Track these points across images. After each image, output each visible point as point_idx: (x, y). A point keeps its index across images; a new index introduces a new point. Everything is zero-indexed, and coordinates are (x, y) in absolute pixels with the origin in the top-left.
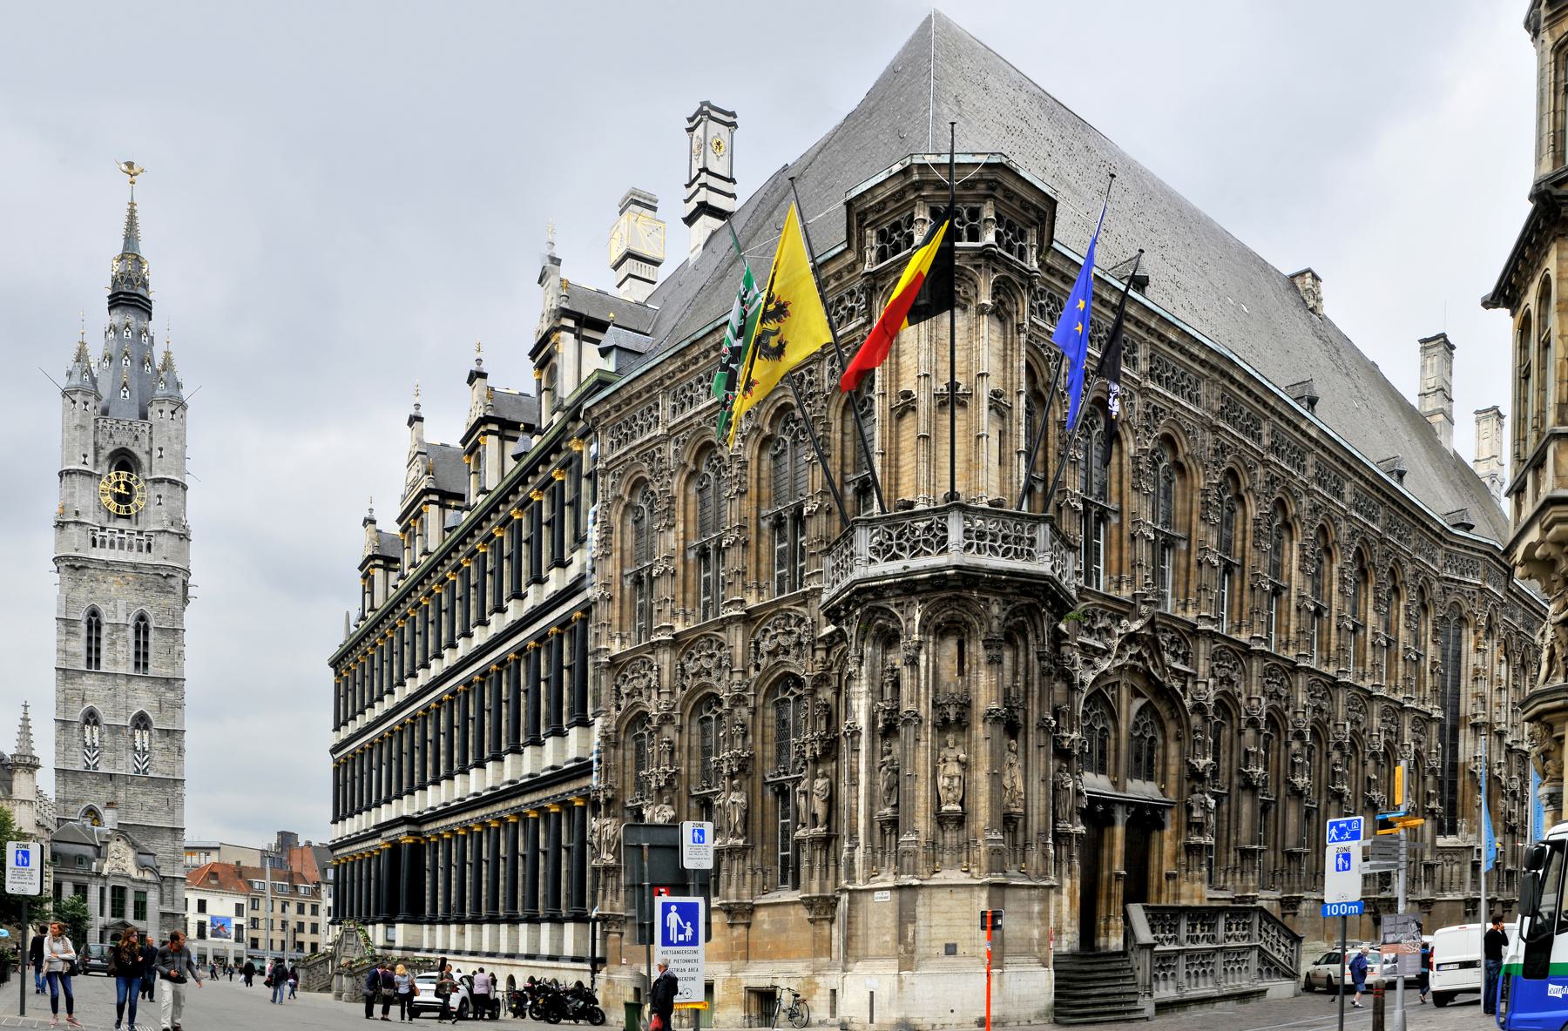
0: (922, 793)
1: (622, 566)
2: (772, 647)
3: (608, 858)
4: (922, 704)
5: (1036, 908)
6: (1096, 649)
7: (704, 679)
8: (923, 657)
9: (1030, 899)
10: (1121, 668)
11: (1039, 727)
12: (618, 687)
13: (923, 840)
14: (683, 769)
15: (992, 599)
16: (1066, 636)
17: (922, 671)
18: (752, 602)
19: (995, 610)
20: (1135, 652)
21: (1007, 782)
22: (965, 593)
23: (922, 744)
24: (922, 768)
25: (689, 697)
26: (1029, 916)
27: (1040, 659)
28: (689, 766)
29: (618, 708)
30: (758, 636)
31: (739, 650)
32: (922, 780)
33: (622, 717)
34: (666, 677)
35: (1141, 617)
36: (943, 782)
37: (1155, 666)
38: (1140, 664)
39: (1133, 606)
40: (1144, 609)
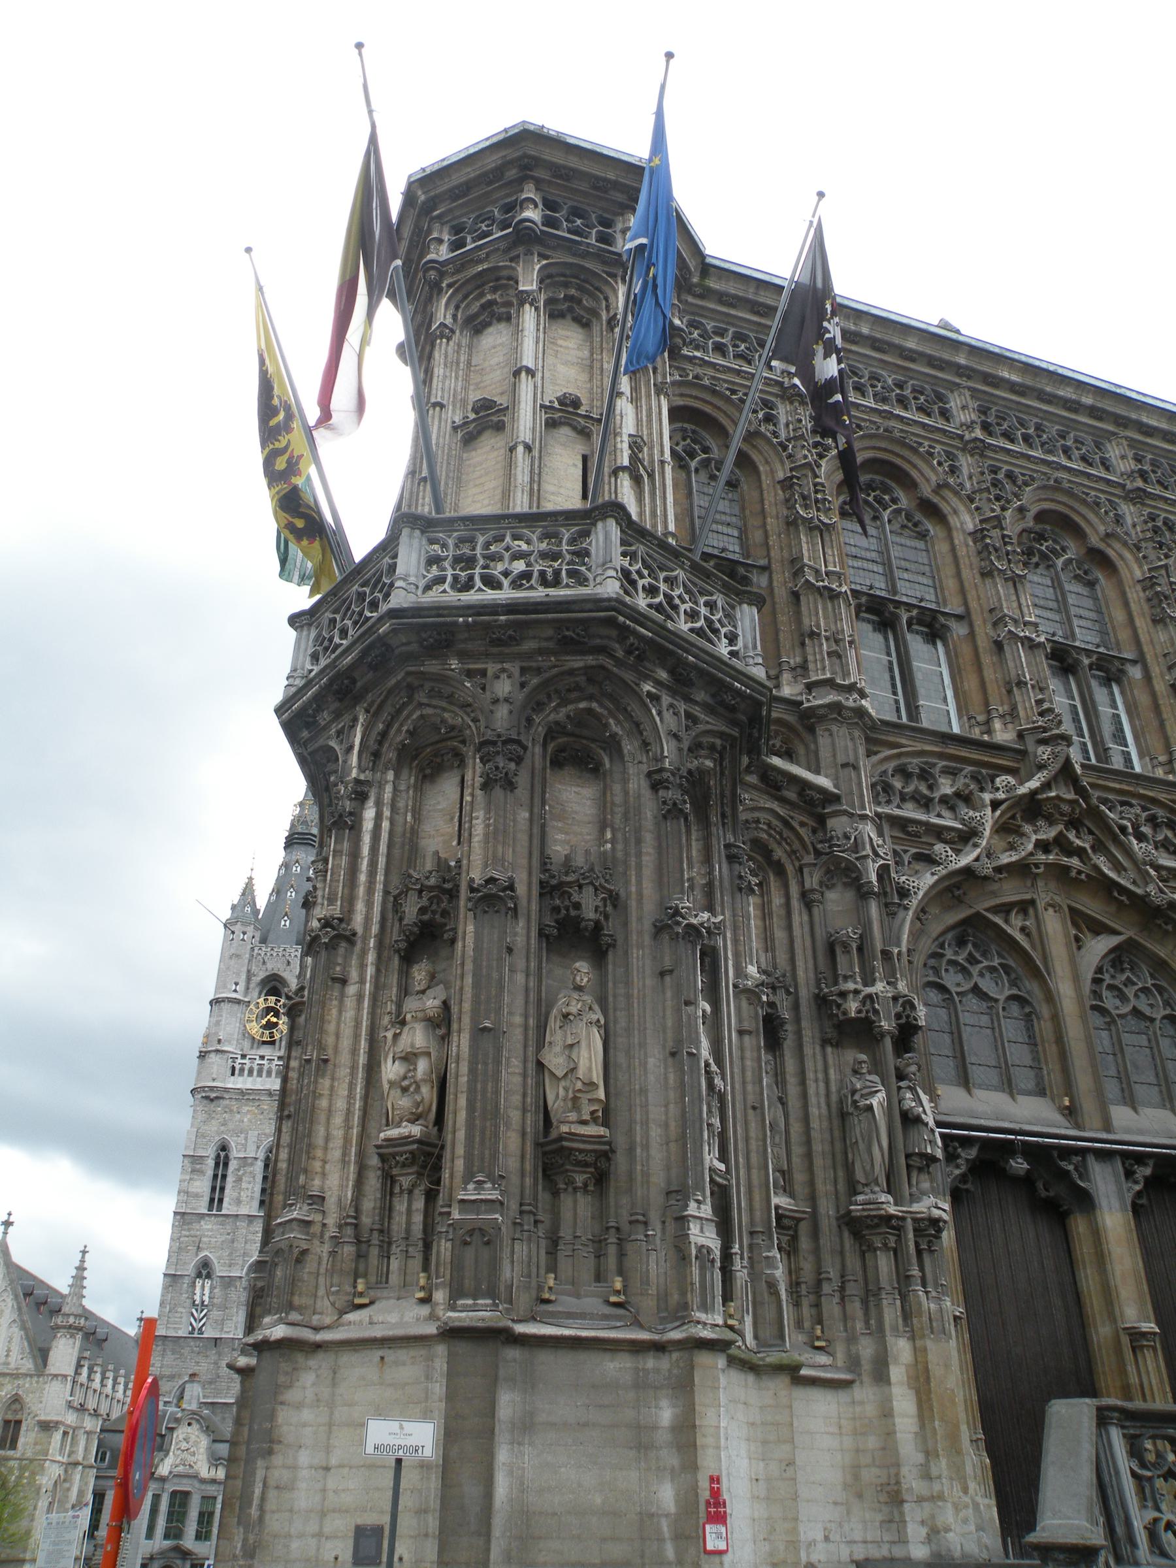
0: (341, 1104)
4: (360, 906)
5: (666, 1414)
6: (939, 833)
8: (369, 814)
9: (641, 1384)
10: (1022, 869)
11: (659, 929)
13: (331, 1220)
15: (492, 668)
16: (836, 799)
17: (366, 839)
19: (504, 687)
20: (1049, 833)
21: (555, 1061)
22: (432, 666)
23: (352, 990)
24: (346, 1043)
26: (641, 1441)
27: (655, 786)
32: (343, 1072)
35: (1041, 767)
36: (391, 1070)
37: (1118, 867)
38: (1075, 862)
39: (1023, 753)
40: (1044, 753)
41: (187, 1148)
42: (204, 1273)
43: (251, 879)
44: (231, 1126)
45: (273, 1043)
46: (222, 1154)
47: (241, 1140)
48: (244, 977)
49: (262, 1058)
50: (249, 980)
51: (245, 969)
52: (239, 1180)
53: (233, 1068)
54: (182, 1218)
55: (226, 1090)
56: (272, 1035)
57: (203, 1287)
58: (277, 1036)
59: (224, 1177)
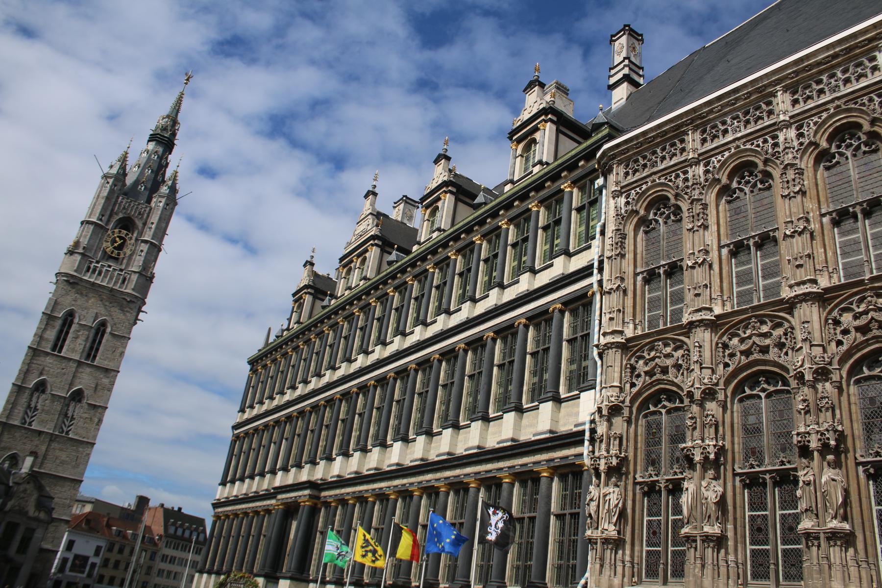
1: (635, 266)
3: (611, 531)
7: (756, 356)
12: (633, 368)
14: (728, 446)
18: (824, 282)
25: (734, 375)
28: (733, 443)
29: (633, 385)
30: (835, 313)
31: (816, 325)
34: (707, 354)
41: (47, 308)
42: (41, 389)
43: (127, 153)
44: (79, 302)
45: (116, 259)
46: (70, 318)
47: (84, 313)
48: (108, 213)
49: (110, 266)
50: (111, 216)
51: (110, 208)
52: (77, 338)
53: (89, 268)
54: (34, 352)
55: (81, 279)
56: (119, 254)
57: (38, 398)
58: (122, 256)
59: (67, 333)
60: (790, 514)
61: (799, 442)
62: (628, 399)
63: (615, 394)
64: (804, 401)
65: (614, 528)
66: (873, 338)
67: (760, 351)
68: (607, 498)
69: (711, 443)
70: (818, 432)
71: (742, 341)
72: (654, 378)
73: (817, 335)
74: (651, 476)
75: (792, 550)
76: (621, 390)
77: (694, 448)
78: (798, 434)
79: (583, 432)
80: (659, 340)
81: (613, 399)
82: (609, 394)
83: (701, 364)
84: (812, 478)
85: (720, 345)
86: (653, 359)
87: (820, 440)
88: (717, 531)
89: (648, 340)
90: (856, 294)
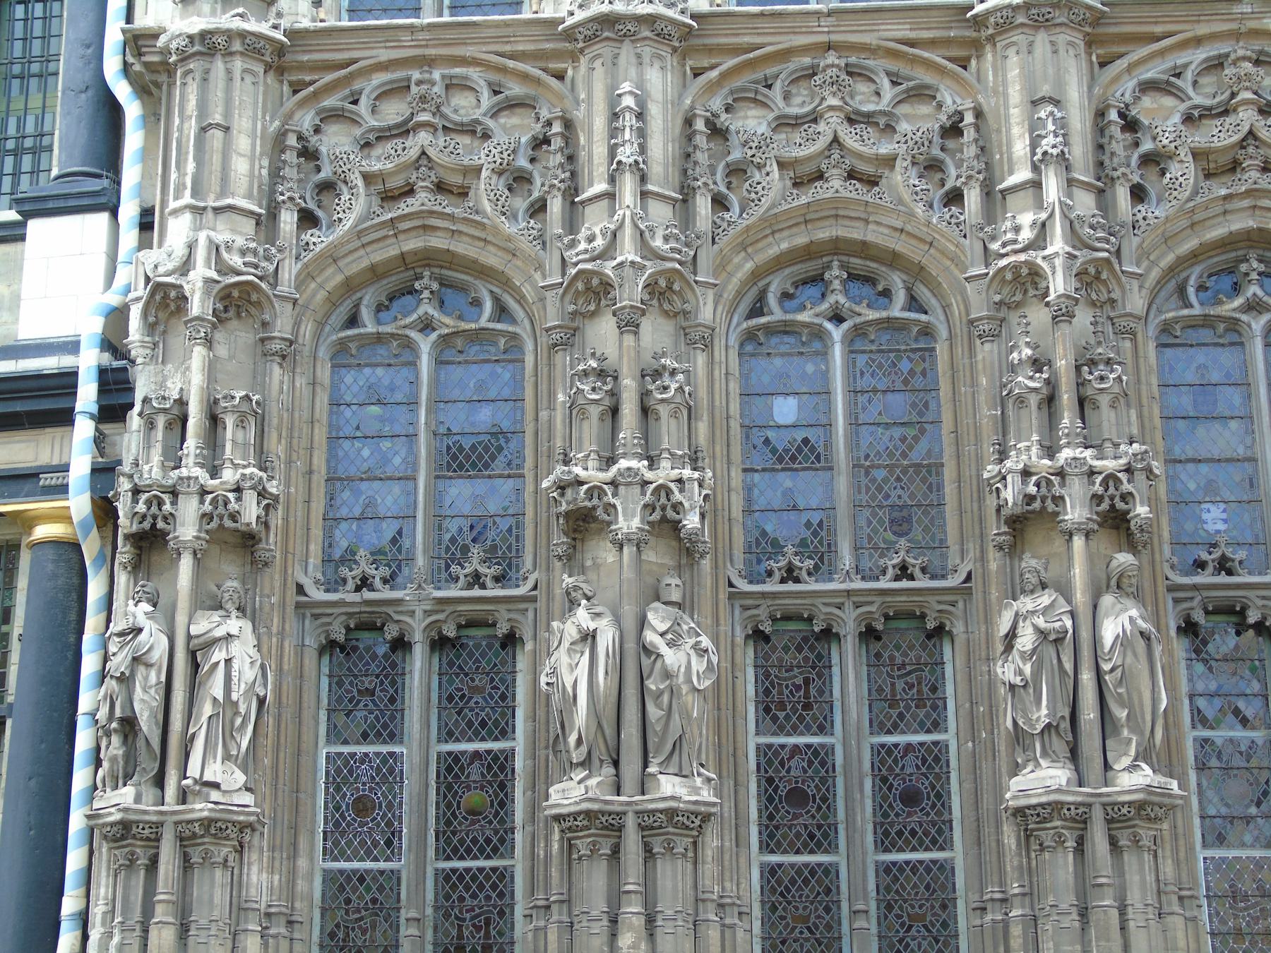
2: (1219, 135)
33: (332, 256)
34: (661, 149)
60: (909, 747)
61: (1030, 499)
62: (290, 271)
63: (240, 241)
64: (1037, 364)
65: (240, 778)
66: (1249, 193)
67: (851, 175)
68: (218, 655)
69: (687, 473)
70: (1092, 473)
71: (784, 123)
72: (404, 207)
73: (1080, 152)
74: (364, 583)
75: (914, 866)
76: (266, 223)
77: (613, 483)
78: (1026, 473)
79: (67, 382)
80: (427, 62)
81: (236, 260)
82: (221, 237)
83: (643, 179)
84: (1069, 623)
85: (700, 125)
86: (404, 130)
87: (1097, 498)
88: (707, 795)
89: (384, 55)
90: (1198, 41)
